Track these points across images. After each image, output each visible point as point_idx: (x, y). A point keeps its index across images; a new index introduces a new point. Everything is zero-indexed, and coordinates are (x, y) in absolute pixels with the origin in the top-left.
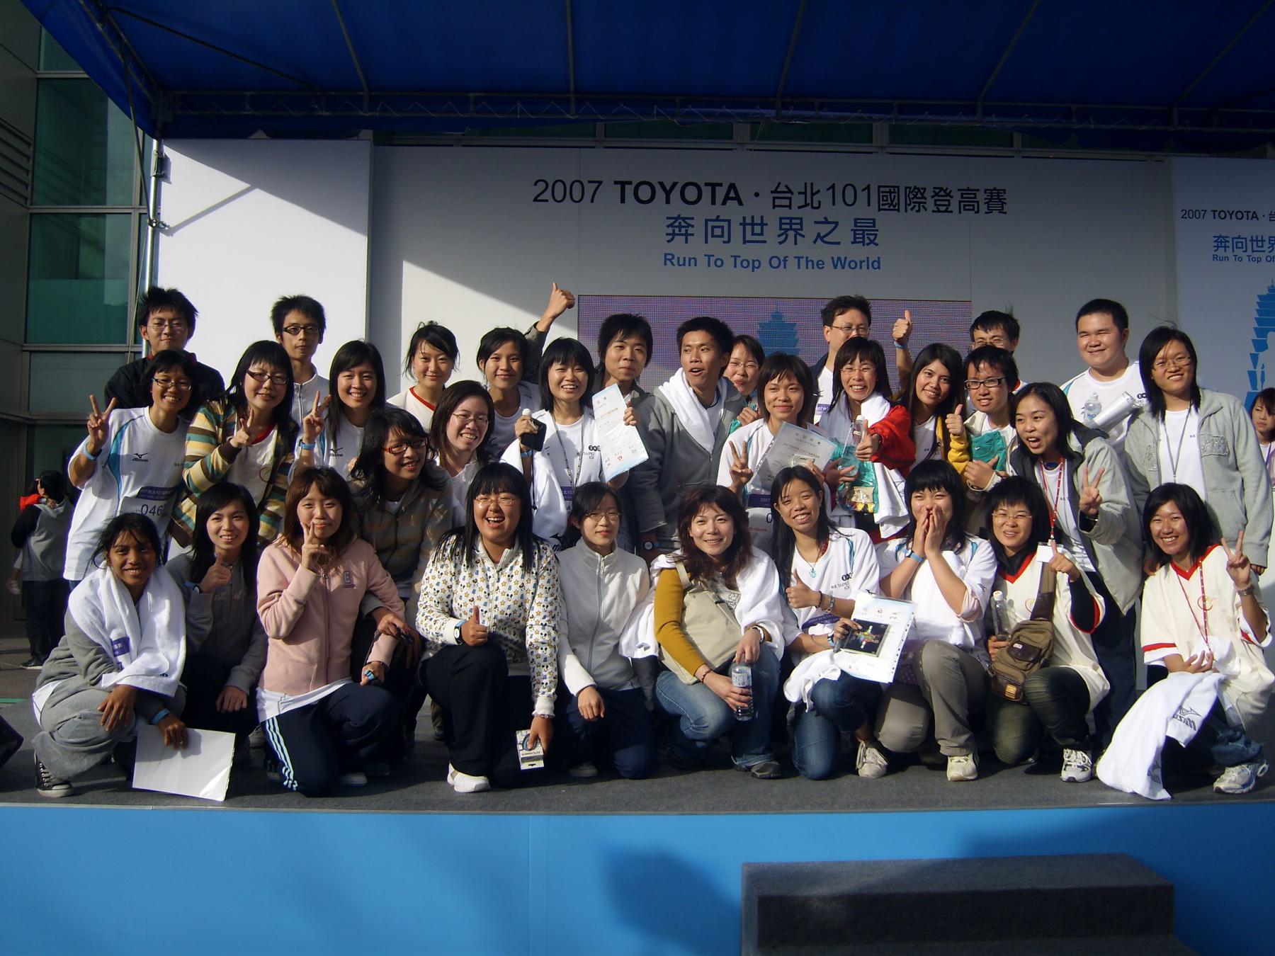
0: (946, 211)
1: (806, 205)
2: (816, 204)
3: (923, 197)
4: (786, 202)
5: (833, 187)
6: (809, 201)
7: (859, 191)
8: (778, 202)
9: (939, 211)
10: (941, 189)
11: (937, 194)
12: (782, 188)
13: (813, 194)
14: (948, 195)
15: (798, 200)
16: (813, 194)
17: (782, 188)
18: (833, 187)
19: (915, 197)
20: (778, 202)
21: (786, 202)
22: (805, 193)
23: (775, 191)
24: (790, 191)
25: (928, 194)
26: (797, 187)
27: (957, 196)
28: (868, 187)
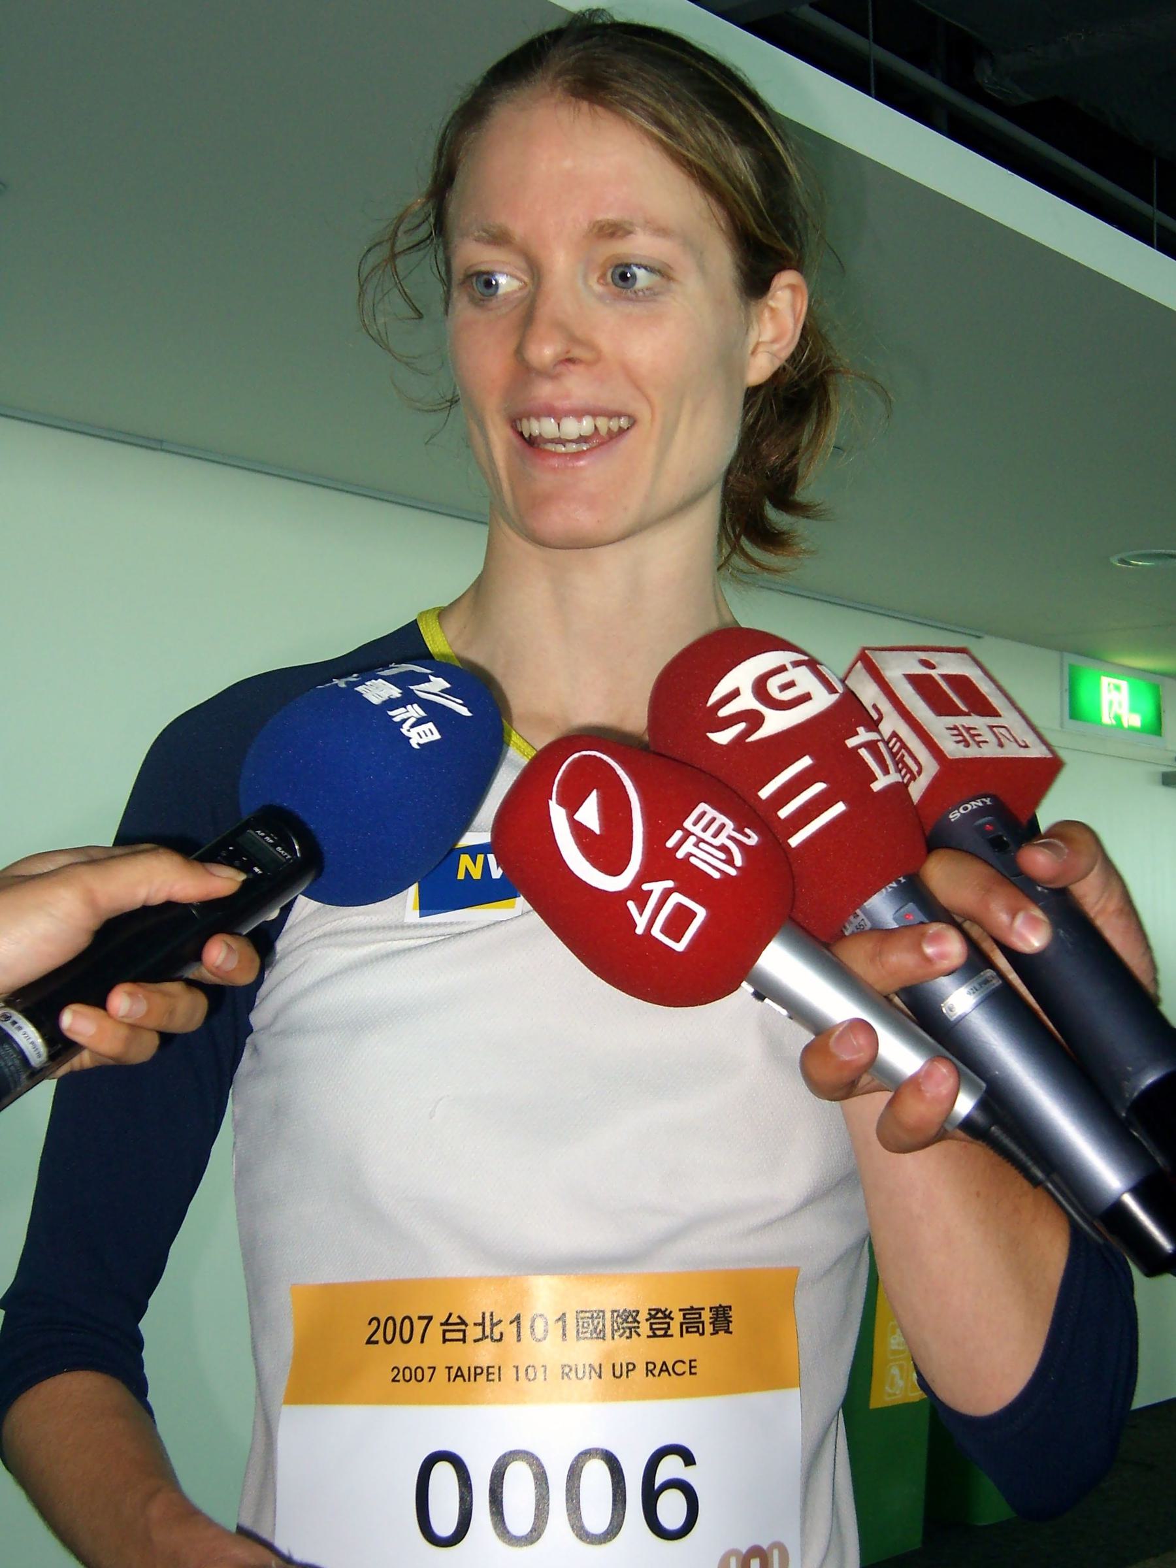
0: (665, 1335)
1: (484, 1337)
2: (497, 1337)
3: (635, 1321)
4: (460, 1335)
5: (518, 1318)
6: (488, 1332)
7: (551, 1322)
8: (449, 1336)
9: (655, 1336)
10: (658, 1311)
11: (654, 1317)
12: (454, 1319)
13: (493, 1325)
14: (669, 1316)
15: (474, 1332)
16: (493, 1325)
17: (454, 1319)
18: (518, 1318)
19: (626, 1321)
20: (449, 1336)
21: (460, 1335)
22: (483, 1324)
23: (446, 1323)
24: (463, 1323)
25: (642, 1317)
26: (472, 1317)
27: (678, 1317)
28: (562, 1318)
